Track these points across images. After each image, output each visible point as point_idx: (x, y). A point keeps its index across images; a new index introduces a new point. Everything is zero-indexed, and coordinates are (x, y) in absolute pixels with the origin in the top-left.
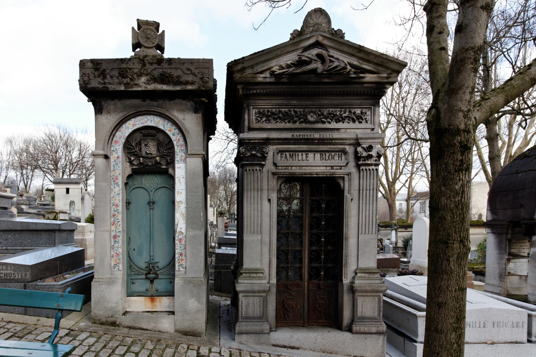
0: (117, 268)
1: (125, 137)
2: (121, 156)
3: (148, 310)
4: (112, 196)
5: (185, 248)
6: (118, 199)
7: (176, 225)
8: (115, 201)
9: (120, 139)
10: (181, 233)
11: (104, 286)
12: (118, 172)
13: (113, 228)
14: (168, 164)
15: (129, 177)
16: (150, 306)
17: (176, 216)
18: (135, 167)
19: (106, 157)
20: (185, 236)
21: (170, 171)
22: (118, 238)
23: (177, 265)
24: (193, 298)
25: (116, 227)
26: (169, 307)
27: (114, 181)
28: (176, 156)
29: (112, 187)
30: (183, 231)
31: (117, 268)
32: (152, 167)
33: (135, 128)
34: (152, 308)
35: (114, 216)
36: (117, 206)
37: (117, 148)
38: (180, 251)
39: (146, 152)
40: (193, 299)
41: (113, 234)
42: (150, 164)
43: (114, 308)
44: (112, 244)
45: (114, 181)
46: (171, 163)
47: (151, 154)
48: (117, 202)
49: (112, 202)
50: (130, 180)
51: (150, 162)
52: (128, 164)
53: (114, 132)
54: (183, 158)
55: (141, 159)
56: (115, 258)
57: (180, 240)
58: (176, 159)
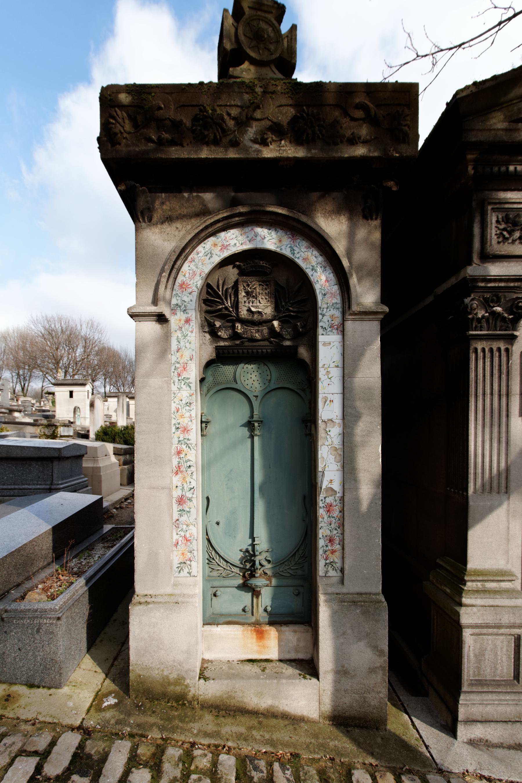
1: (204, 275)
2: (193, 318)
4: (173, 409)
5: (342, 525)
6: (188, 414)
7: (320, 474)
8: (181, 420)
9: (191, 279)
12: (187, 354)
13: (176, 480)
14: (297, 336)
15: (209, 364)
16: (255, 648)
17: (320, 452)
18: (222, 344)
19: (161, 319)
20: (342, 499)
21: (303, 352)
23: (321, 563)
25: (184, 479)
27: (179, 375)
28: (320, 317)
29: (174, 388)
30: (337, 486)
31: (186, 570)
32: (261, 343)
33: (226, 254)
34: (260, 652)
35: (179, 453)
36: (186, 430)
37: (185, 299)
38: (328, 533)
39: (249, 310)
42: (258, 336)
44: (176, 516)
45: (179, 375)
47: (259, 313)
48: (184, 422)
49: (173, 422)
50: (210, 372)
51: (258, 331)
52: (208, 336)
53: (179, 262)
54: (337, 321)
55: (238, 325)
56: (181, 547)
57: (329, 508)
58: (320, 324)
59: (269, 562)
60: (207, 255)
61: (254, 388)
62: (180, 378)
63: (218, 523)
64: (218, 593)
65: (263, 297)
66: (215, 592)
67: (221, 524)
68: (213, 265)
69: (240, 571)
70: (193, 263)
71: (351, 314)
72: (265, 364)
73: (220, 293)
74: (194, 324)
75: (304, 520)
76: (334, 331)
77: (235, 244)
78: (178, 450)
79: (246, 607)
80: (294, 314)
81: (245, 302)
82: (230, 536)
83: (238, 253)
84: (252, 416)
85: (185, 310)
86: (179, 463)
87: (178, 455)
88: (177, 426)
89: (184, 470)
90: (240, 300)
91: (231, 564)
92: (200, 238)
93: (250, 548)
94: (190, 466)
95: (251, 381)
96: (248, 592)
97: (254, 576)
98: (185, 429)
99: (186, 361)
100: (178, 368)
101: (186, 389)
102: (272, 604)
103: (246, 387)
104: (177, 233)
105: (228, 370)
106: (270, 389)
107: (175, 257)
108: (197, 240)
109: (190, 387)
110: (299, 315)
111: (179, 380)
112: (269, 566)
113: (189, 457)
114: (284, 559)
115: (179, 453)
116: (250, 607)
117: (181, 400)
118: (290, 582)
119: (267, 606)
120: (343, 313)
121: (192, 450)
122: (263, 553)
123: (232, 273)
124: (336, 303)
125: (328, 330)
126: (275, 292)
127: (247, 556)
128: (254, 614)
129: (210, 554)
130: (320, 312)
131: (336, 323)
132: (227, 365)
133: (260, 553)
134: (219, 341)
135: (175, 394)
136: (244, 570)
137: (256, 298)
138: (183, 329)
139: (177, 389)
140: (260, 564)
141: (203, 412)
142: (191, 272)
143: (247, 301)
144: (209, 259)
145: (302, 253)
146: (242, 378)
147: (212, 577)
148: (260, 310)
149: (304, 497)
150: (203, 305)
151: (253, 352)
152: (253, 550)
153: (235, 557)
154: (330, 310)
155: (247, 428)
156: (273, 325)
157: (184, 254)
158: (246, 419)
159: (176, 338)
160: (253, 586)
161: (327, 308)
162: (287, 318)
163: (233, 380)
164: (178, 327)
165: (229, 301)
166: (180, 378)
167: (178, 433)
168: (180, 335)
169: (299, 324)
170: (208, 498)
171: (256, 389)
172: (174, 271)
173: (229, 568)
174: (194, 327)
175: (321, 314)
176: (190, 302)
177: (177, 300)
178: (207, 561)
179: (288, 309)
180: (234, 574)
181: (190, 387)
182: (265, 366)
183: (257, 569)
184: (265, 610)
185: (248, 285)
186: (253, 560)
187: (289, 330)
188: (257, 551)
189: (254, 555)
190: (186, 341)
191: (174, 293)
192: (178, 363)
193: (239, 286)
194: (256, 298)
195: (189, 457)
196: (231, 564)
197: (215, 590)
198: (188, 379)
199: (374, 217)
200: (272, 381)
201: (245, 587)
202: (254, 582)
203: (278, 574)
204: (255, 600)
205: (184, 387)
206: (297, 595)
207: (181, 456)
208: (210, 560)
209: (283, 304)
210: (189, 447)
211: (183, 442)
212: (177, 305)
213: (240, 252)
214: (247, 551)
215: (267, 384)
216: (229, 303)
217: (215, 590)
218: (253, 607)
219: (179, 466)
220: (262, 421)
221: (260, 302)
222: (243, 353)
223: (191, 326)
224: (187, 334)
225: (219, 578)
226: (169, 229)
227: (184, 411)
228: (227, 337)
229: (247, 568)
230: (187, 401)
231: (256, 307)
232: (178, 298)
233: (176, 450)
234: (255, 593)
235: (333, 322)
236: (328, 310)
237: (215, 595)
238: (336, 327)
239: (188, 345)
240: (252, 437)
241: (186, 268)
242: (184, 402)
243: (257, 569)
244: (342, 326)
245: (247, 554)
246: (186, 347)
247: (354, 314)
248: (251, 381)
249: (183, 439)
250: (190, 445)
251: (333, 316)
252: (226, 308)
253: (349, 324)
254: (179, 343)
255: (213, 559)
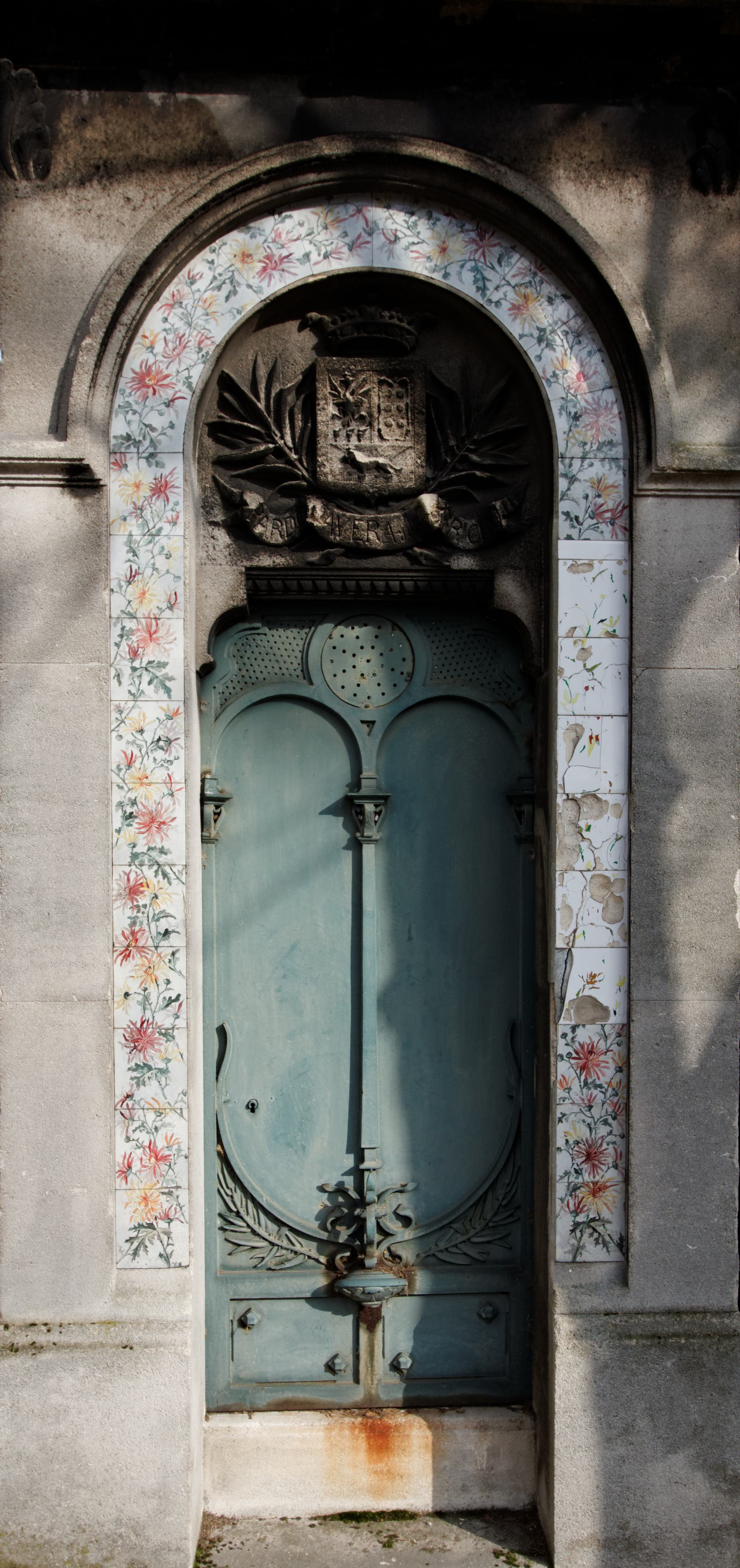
0: (155, 1249)
1: (210, 348)
2: (178, 480)
3: (349, 1505)
4: (116, 757)
5: (623, 1111)
6: (160, 775)
7: (559, 958)
8: (139, 793)
9: (173, 356)
10: (593, 1008)
11: (69, 1381)
12: (158, 589)
13: (126, 975)
14: (491, 541)
15: (225, 624)
16: (365, 1479)
17: (559, 892)
18: (266, 561)
19: (79, 479)
20: (625, 1031)
21: (511, 591)
22: (163, 1045)
23: (562, 1224)
24: (673, 1448)
25: (149, 970)
26: (487, 1483)
27: (134, 654)
28: (562, 484)
29: (119, 693)
30: (608, 994)
31: (155, 1249)
32: (386, 561)
33: (278, 285)
34: (377, 1492)
35: (133, 891)
36: (154, 822)
37: (154, 420)
38: (583, 1133)
39: (349, 460)
40: (679, 1461)
41: (127, 1015)
42: (373, 538)
43: (137, 1529)
44: (123, 1083)
45: (134, 654)
46: (527, 540)
48: (151, 796)
49: (117, 796)
50: (228, 648)
51: (375, 524)
52: (223, 537)
53: (134, 306)
54: (614, 499)
55: (316, 506)
56: (141, 1180)
57: (585, 1057)
58: (563, 506)
59: (406, 1221)
60: (219, 288)
61: (362, 697)
62: (137, 664)
63: (252, 1108)
64: (253, 1318)
65: (391, 421)
66: (244, 1315)
67: (261, 1110)
68: (239, 317)
69: (320, 1251)
70: (178, 311)
71: (654, 478)
72: (395, 626)
73: (261, 405)
74: (181, 499)
75: (511, 1097)
76: (603, 527)
77: (307, 256)
78: (132, 883)
79: (336, 1356)
80: (485, 475)
81: (336, 435)
82: (289, 1145)
83: (315, 282)
84: (356, 783)
85: (152, 455)
86: (133, 924)
87: (132, 899)
88: (129, 810)
89: (150, 943)
90: (321, 427)
91: (292, 1229)
92: (198, 232)
93: (349, 1182)
94: (167, 933)
95: (353, 677)
96: (344, 1313)
97: (361, 1266)
98: (153, 820)
99: (156, 611)
100: (132, 632)
101: (155, 697)
102: (413, 1348)
103: (340, 693)
104: (126, 215)
105: (283, 643)
106: (407, 702)
107: (121, 290)
108: (188, 240)
109: (168, 691)
110: (500, 477)
111: (134, 669)
112: (408, 1234)
113: (163, 905)
114: (453, 1212)
115: (133, 891)
116: (350, 1359)
117: (141, 731)
118: (468, 1281)
119: (399, 1355)
120: (632, 475)
121: (175, 882)
122: (387, 1197)
123: (297, 344)
124: (611, 443)
125: (586, 525)
126: (428, 408)
127: (339, 1206)
128: (362, 1376)
129: (228, 1200)
130: (561, 468)
131: (610, 505)
132: (282, 625)
133: (379, 1196)
134: (255, 553)
135: (121, 712)
136: (331, 1249)
137: (371, 425)
138: (147, 514)
139: (127, 696)
140: (381, 1229)
141: (206, 768)
142: (170, 337)
143: (343, 433)
144: (227, 298)
145: (509, 288)
146: (327, 666)
147: (235, 1268)
148: (381, 460)
149: (513, 1028)
150: (208, 442)
151: (359, 588)
152: (360, 1186)
153: (305, 1207)
154: (591, 465)
155: (341, 820)
156: (420, 507)
157: (149, 282)
158: (337, 793)
159: (125, 539)
160: (358, 1293)
161: (583, 458)
162: (464, 488)
163: (299, 672)
164: (131, 507)
165: (288, 431)
166: (137, 664)
167: (131, 831)
168: (136, 532)
169: (498, 504)
170: (222, 1032)
171: (368, 702)
172: (119, 333)
173: (285, 1243)
174: (180, 508)
175: (565, 476)
176: (169, 431)
177: (129, 423)
178: (219, 1222)
179: (465, 459)
180: (299, 1260)
181: (168, 691)
182: (397, 633)
183: (371, 1243)
184: (395, 1366)
185: (346, 384)
186: (358, 1217)
187: (470, 522)
188: (371, 1189)
189: (363, 1203)
190: (156, 550)
191: (119, 400)
192: (132, 616)
193: (319, 385)
194: (371, 425)
195: (163, 905)
196: (292, 1229)
197: (242, 1307)
198: (163, 665)
199: (724, 186)
200: (418, 678)
201: (334, 1297)
202: (359, 1282)
203: (432, 1260)
204: (364, 1336)
205: (149, 690)
206: (488, 1321)
207: (141, 903)
208: (228, 1219)
209: (452, 443)
210: (165, 875)
211: (146, 859)
212: (128, 437)
213: (322, 281)
214: (340, 1190)
215: (403, 685)
216: (288, 438)
217: (242, 1307)
218: (357, 1357)
219: (133, 933)
220: (386, 798)
221: (381, 437)
222: (331, 590)
223: (171, 505)
224: (160, 529)
225: (254, 1271)
226: (102, 203)
227: (149, 763)
228: (280, 540)
229: (341, 1240)
230: (160, 733)
231: (371, 451)
232: (130, 416)
233: (123, 884)
234: (366, 1316)
235: (600, 501)
236: (587, 462)
237: (243, 1323)
238: (608, 515)
239: (160, 561)
240: (356, 846)
241: (153, 323)
242: (149, 736)
243: (371, 1243)
244: (626, 512)
245: (341, 1199)
246: (156, 569)
247: (664, 476)
248: (353, 677)
249: (145, 850)
250: (167, 869)
251: (599, 481)
252: (279, 453)
253: (647, 508)
254: (135, 555)
255: (238, 1214)
